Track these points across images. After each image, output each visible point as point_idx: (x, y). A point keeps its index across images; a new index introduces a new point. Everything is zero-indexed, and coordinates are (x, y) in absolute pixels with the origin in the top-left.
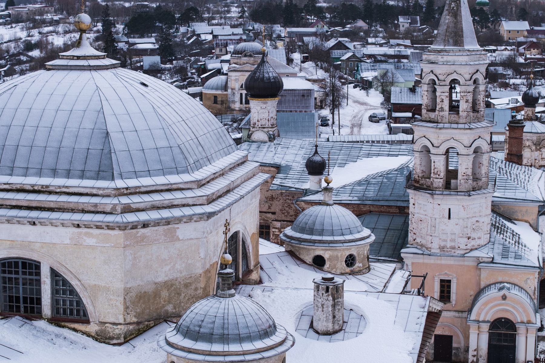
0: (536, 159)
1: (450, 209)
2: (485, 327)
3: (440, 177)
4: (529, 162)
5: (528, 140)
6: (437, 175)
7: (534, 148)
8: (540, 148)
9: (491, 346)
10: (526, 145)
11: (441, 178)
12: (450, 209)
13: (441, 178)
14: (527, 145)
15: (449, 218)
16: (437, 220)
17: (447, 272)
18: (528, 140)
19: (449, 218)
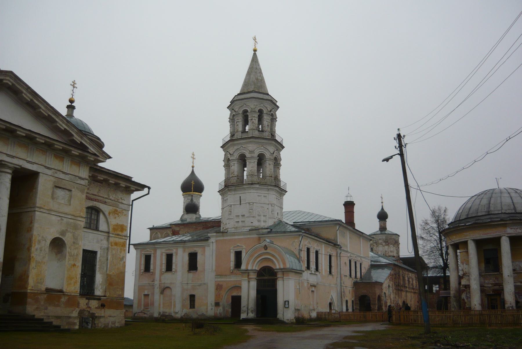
0: (386, 251)
1: (240, 197)
2: (253, 276)
3: (235, 176)
4: (382, 253)
5: (380, 239)
6: (233, 174)
7: (384, 244)
8: (389, 244)
9: (258, 291)
10: (379, 242)
11: (235, 177)
12: (240, 197)
13: (235, 177)
14: (380, 242)
15: (240, 204)
16: (232, 206)
17: (239, 245)
18: (380, 239)
19: (240, 204)
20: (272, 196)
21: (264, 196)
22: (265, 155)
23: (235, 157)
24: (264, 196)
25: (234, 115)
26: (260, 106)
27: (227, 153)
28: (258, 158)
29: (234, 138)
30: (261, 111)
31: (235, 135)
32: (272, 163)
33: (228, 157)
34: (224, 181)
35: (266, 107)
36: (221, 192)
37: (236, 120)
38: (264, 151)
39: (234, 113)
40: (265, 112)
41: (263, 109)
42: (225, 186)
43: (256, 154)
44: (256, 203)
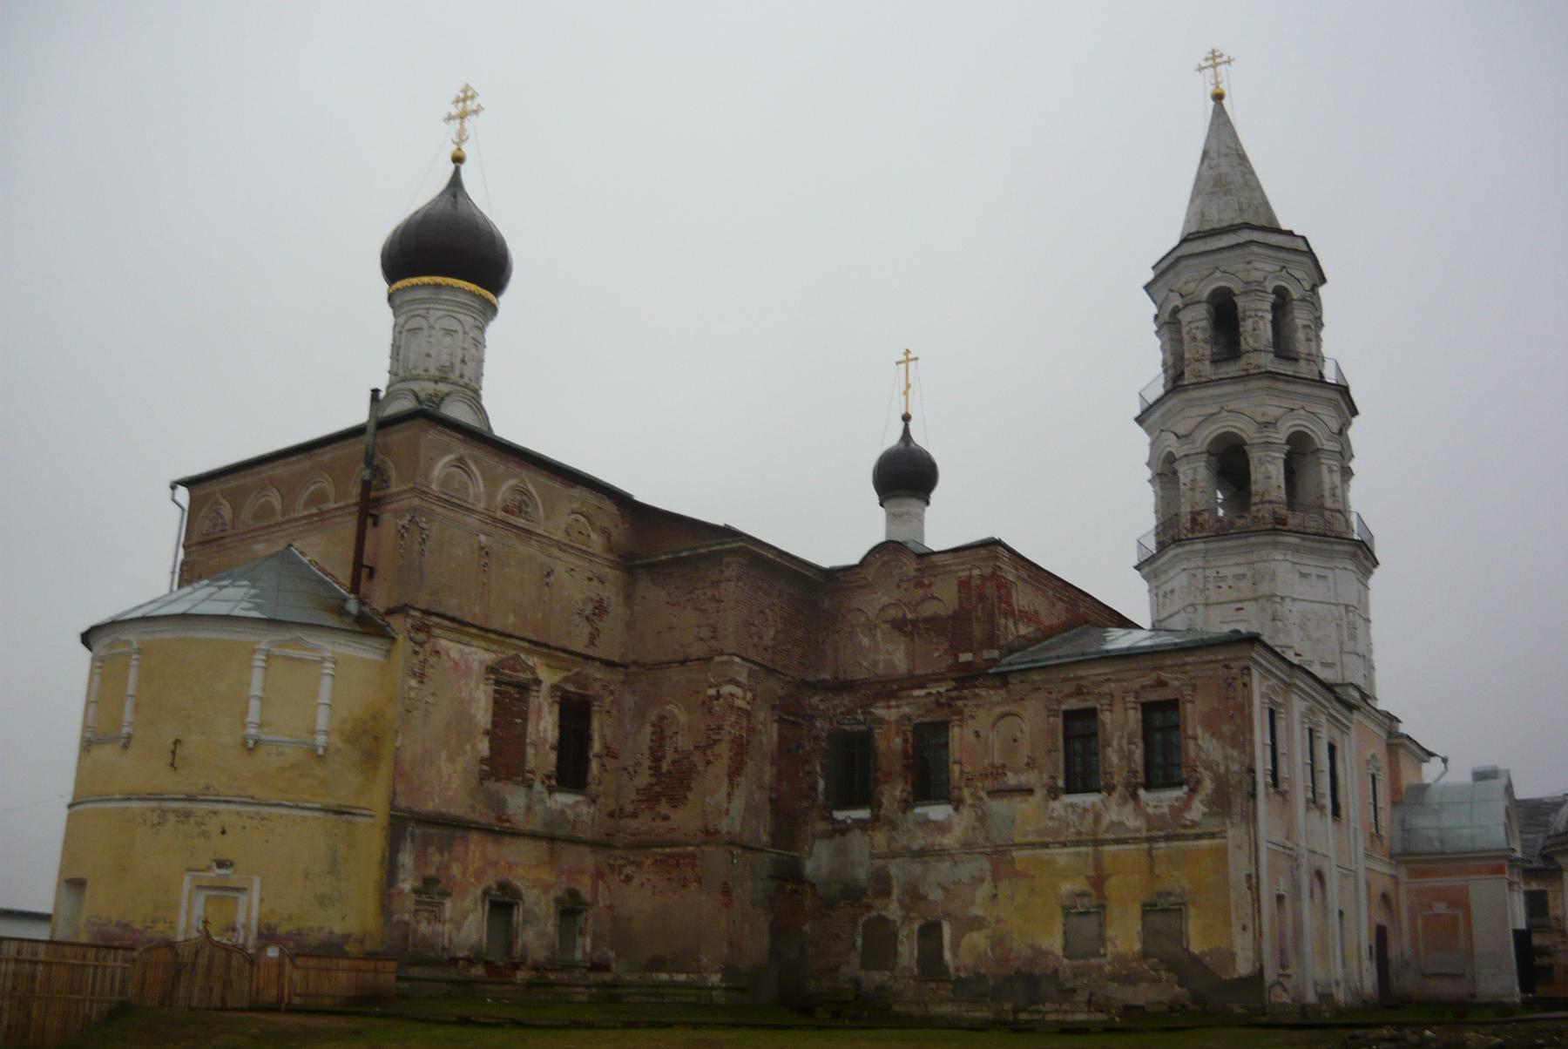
20: (1343, 576)
21: (1319, 577)
22: (1313, 438)
23: (1198, 444)
24: (1319, 577)
25: (1176, 310)
26: (1277, 278)
27: (1163, 433)
28: (1287, 447)
29: (1186, 382)
30: (1282, 296)
31: (1186, 375)
32: (1335, 464)
33: (1168, 449)
34: (1154, 532)
35: (1298, 280)
36: (1146, 569)
37: (1183, 324)
38: (1306, 424)
39: (1178, 302)
40: (1295, 297)
41: (1289, 288)
42: (1162, 546)
43: (1281, 435)
44: (1294, 599)
